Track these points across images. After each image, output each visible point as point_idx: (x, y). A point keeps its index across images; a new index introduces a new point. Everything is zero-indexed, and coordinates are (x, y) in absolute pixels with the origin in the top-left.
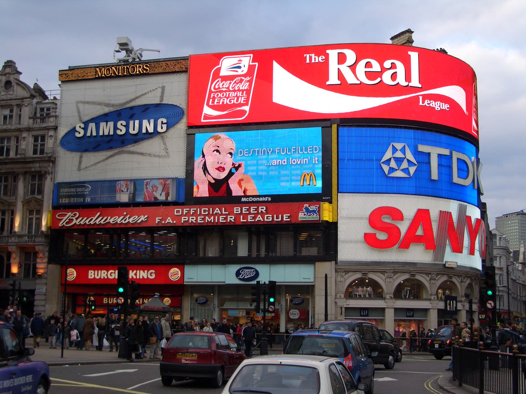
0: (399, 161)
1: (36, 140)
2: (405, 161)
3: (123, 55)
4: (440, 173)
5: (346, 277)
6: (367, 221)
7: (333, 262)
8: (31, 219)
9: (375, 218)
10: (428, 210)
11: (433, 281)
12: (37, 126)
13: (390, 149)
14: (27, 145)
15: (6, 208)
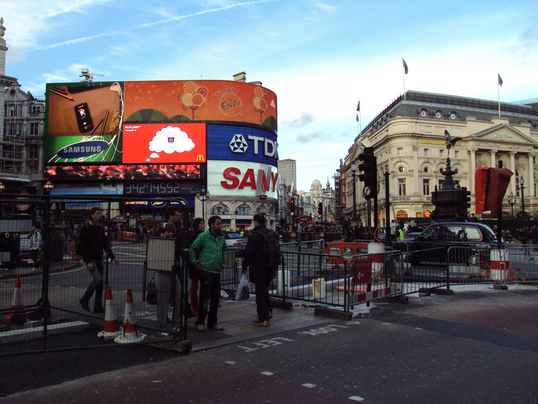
0: (239, 144)
2: (242, 144)
3: (84, 79)
4: (259, 150)
9: (226, 174)
12: (33, 118)
14: (27, 128)
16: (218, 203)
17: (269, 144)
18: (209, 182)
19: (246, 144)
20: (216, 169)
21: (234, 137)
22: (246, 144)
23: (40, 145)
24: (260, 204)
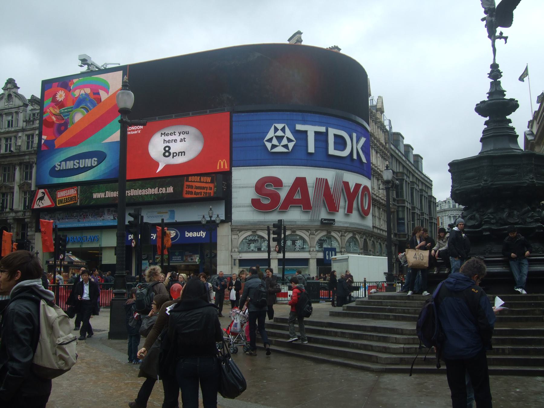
0: (280, 139)
1: (28, 138)
4: (316, 147)
5: (240, 234)
6: (253, 189)
7: (230, 223)
8: (25, 199)
9: (261, 186)
10: (305, 178)
11: (312, 236)
13: (273, 128)
14: (22, 141)
15: (8, 191)
16: (249, 233)
17: (335, 136)
18: (234, 201)
19: (291, 137)
20: (245, 180)
21: (273, 128)
22: (293, 139)
23: (33, 163)
24: (324, 233)
